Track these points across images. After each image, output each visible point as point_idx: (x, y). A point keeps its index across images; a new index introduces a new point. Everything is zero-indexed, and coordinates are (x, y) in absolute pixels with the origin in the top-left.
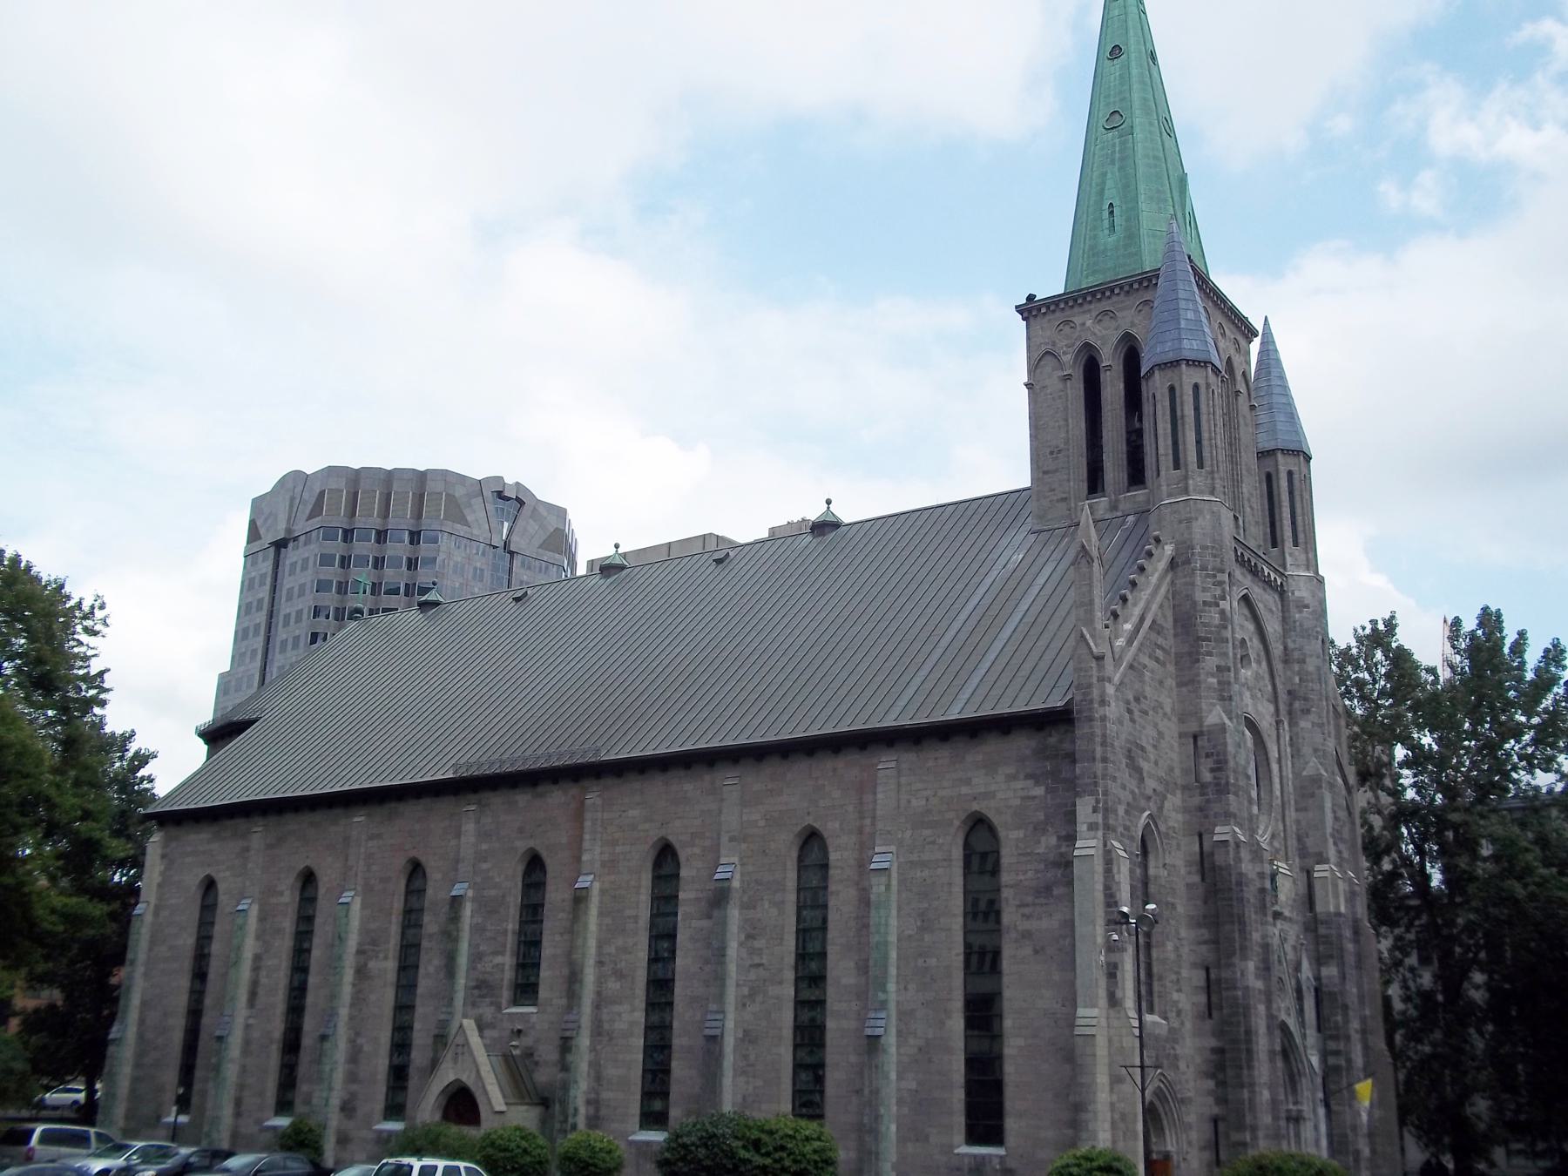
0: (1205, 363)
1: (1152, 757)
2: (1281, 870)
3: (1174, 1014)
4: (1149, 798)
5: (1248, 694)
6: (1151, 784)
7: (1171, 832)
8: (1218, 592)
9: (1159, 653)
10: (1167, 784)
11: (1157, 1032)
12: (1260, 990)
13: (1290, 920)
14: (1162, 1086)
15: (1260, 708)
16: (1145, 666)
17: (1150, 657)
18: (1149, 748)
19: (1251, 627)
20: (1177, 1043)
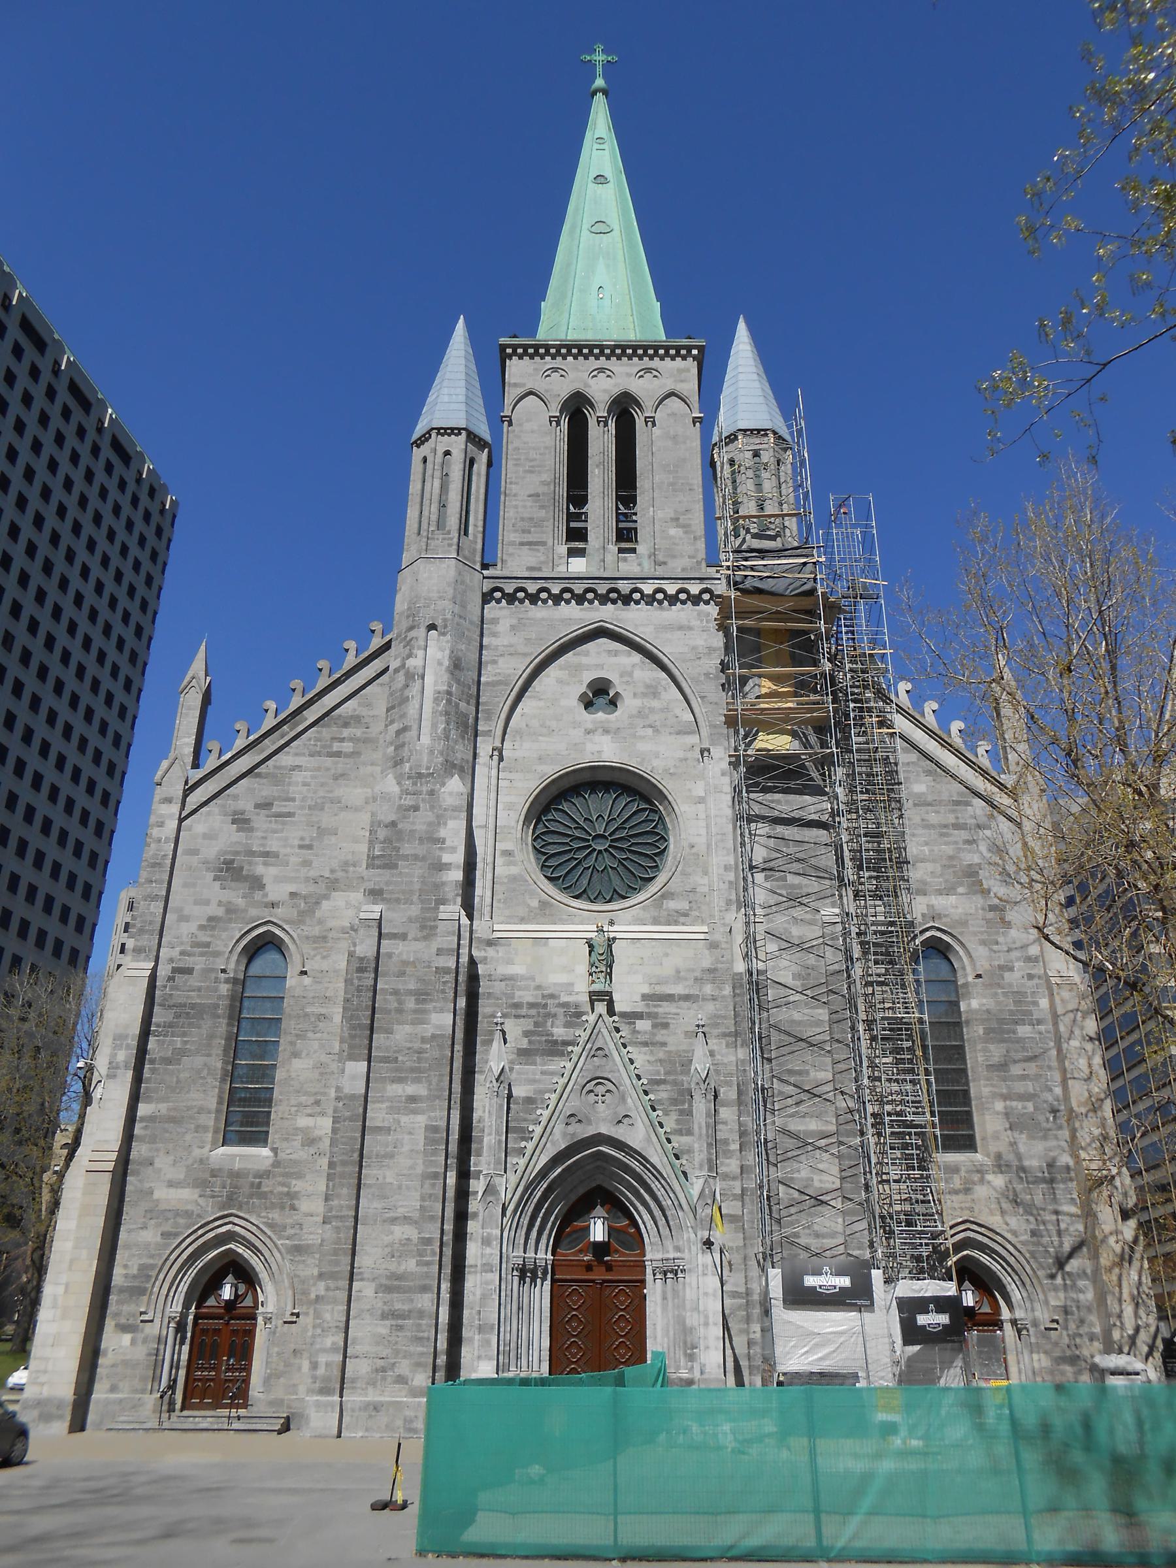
0: (429, 432)
1: (293, 860)
2: (612, 935)
3: (297, 1144)
4: (273, 905)
5: (606, 739)
6: (276, 891)
7: (331, 935)
8: (407, 651)
9: (347, 747)
10: (337, 880)
11: (237, 1166)
12: (412, 1099)
13: (687, 998)
14: (237, 1229)
15: (643, 747)
16: (298, 767)
17: (311, 755)
18: (283, 851)
19: (637, 657)
20: (300, 1176)
